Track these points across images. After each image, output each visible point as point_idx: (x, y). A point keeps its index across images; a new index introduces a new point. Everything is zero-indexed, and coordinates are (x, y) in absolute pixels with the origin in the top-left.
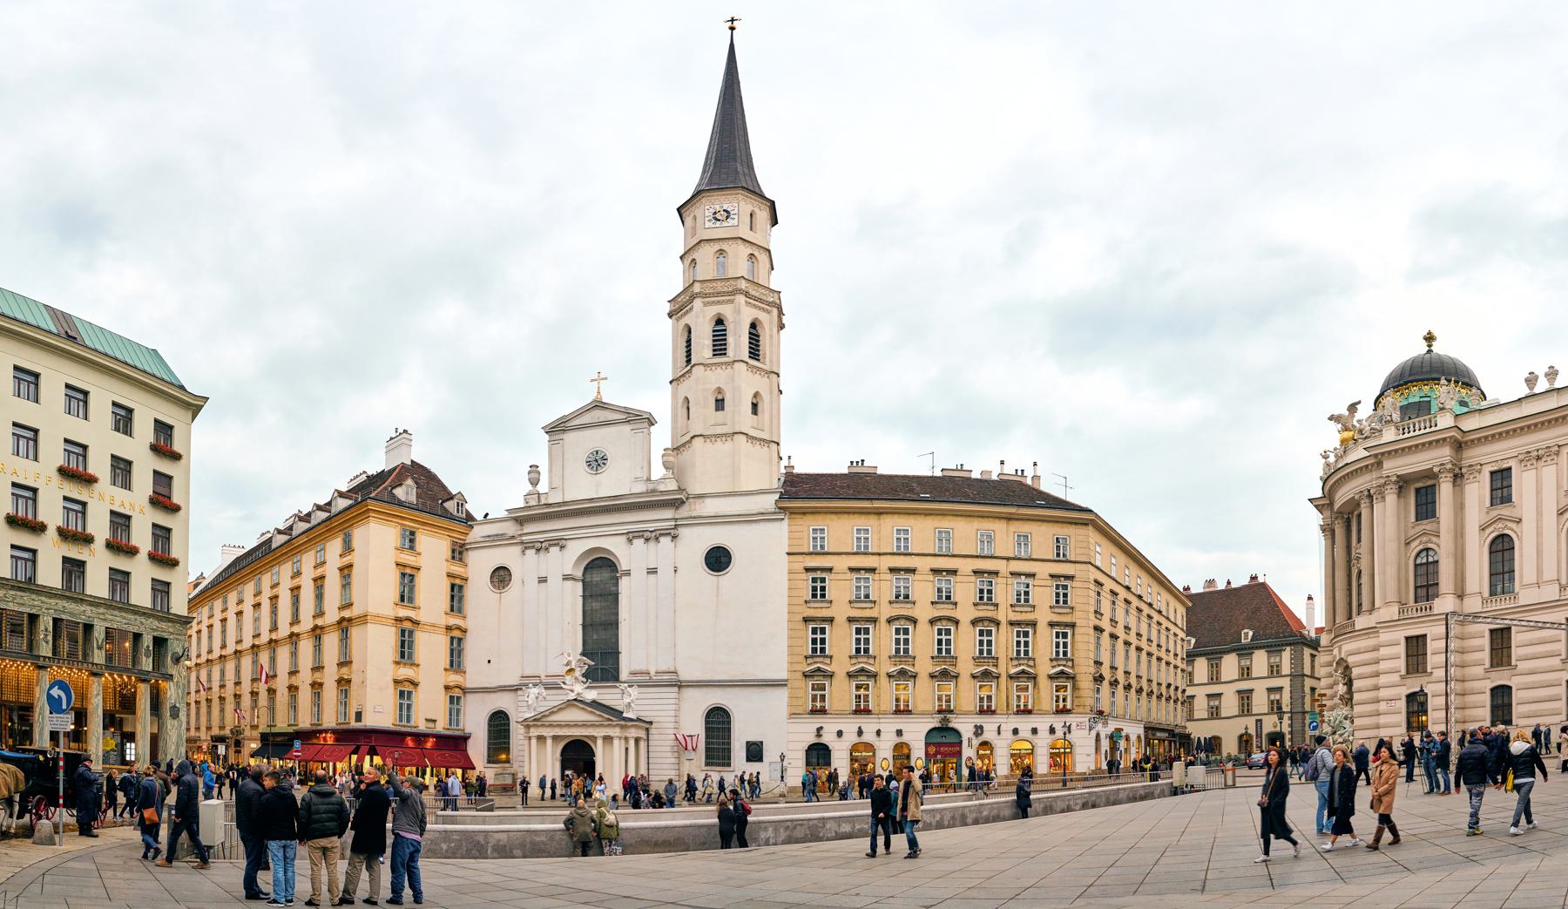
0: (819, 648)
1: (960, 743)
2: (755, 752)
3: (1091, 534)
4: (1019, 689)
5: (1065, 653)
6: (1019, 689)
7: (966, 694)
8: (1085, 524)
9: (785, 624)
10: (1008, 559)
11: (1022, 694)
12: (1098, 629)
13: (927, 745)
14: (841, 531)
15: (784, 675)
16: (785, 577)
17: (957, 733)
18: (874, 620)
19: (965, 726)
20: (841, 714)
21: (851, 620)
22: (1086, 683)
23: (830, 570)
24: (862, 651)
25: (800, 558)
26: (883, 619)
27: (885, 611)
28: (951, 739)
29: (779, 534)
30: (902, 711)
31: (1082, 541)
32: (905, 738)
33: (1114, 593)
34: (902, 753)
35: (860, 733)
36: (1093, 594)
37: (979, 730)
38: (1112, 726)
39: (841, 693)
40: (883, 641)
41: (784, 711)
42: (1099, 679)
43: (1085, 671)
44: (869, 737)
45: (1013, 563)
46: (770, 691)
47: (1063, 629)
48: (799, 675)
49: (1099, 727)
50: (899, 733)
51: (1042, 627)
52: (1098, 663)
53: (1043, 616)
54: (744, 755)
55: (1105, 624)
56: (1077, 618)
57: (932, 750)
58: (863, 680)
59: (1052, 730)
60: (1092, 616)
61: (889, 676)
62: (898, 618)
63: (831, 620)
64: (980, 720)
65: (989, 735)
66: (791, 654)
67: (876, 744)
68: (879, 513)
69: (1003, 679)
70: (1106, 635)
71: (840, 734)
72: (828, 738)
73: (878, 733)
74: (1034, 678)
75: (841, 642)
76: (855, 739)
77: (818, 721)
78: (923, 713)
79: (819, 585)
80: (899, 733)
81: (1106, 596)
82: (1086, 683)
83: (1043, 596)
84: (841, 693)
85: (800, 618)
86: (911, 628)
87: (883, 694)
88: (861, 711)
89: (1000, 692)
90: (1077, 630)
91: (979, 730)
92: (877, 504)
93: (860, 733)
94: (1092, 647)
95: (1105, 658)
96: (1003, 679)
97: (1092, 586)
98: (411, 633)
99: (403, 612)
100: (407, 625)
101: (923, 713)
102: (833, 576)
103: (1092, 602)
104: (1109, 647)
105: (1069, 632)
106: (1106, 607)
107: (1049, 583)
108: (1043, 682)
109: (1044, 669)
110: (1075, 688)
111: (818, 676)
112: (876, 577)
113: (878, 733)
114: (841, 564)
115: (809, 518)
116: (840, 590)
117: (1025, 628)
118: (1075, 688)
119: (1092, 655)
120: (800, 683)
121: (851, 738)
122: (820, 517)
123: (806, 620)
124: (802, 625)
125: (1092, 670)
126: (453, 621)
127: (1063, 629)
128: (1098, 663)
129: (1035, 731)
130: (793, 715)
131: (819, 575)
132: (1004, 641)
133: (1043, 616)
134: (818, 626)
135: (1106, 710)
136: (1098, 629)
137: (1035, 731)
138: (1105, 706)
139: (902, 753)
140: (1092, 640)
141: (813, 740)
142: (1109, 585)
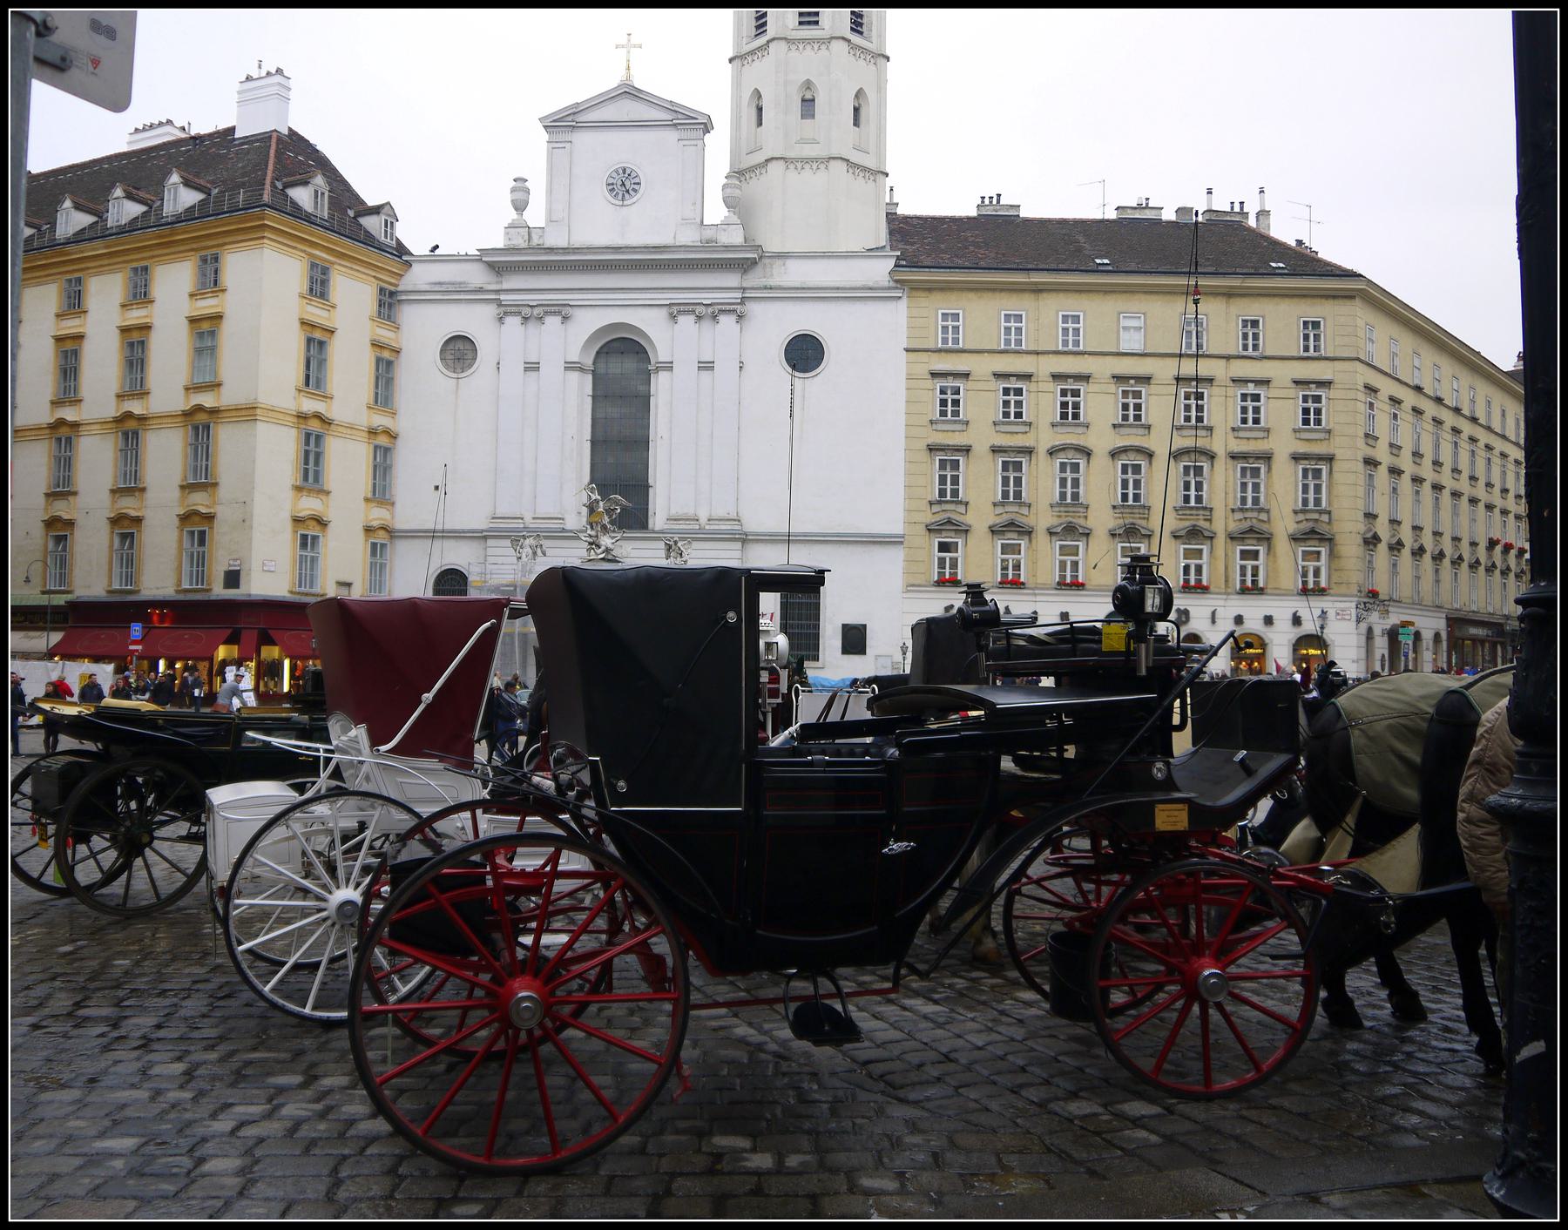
0: (949, 493)
2: (854, 639)
3: (1358, 314)
4: (1245, 555)
5: (1317, 501)
6: (1245, 555)
8: (1349, 296)
9: (902, 454)
11: (1249, 563)
12: (1371, 463)
14: (982, 317)
15: (897, 528)
16: (903, 384)
18: (1029, 451)
21: (996, 450)
22: (1351, 547)
23: (966, 375)
24: (1012, 493)
25: (924, 357)
27: (1045, 438)
29: (892, 323)
31: (1344, 324)
33: (1395, 401)
36: (1362, 407)
38: (1394, 619)
40: (1042, 481)
41: (898, 581)
42: (1372, 541)
43: (1349, 528)
46: (877, 550)
47: (1314, 465)
48: (921, 529)
49: (1374, 617)
51: (1281, 463)
52: (1370, 516)
53: (1283, 443)
54: (838, 643)
55: (1382, 453)
56: (1337, 447)
58: (1012, 539)
59: (1297, 620)
60: (1361, 442)
62: (1063, 449)
63: (967, 450)
66: (908, 498)
68: (1037, 290)
69: (1221, 540)
70: (1383, 471)
74: (1267, 539)
75: (981, 484)
79: (950, 397)
81: (1382, 405)
82: (1351, 547)
83: (1281, 412)
85: (923, 445)
89: (1219, 560)
90: (1337, 466)
92: (1036, 278)
94: (1361, 491)
95: (1382, 507)
96: (1221, 540)
97: (1361, 396)
98: (319, 438)
99: (310, 405)
100: (315, 426)
101: (1099, 589)
102: (970, 385)
103: (1361, 419)
104: (1387, 490)
105: (1324, 469)
106: (1382, 426)
107: (1291, 393)
108: (1282, 544)
110: (1332, 555)
112: (1033, 386)
114: (982, 367)
115: (937, 297)
116: (982, 405)
117: (1253, 463)
119: (1361, 504)
122: (953, 296)
123: (932, 449)
124: (925, 456)
125: (1361, 527)
126: (380, 420)
127: (1314, 465)
128: (1370, 516)
129: (1269, 620)
130: (911, 587)
131: (950, 383)
132: (1222, 484)
133: (1283, 443)
134: (949, 458)
135: (1384, 593)
136: (1371, 463)
137: (1269, 620)
138: (1382, 585)
140: (1361, 480)
142: (1387, 388)
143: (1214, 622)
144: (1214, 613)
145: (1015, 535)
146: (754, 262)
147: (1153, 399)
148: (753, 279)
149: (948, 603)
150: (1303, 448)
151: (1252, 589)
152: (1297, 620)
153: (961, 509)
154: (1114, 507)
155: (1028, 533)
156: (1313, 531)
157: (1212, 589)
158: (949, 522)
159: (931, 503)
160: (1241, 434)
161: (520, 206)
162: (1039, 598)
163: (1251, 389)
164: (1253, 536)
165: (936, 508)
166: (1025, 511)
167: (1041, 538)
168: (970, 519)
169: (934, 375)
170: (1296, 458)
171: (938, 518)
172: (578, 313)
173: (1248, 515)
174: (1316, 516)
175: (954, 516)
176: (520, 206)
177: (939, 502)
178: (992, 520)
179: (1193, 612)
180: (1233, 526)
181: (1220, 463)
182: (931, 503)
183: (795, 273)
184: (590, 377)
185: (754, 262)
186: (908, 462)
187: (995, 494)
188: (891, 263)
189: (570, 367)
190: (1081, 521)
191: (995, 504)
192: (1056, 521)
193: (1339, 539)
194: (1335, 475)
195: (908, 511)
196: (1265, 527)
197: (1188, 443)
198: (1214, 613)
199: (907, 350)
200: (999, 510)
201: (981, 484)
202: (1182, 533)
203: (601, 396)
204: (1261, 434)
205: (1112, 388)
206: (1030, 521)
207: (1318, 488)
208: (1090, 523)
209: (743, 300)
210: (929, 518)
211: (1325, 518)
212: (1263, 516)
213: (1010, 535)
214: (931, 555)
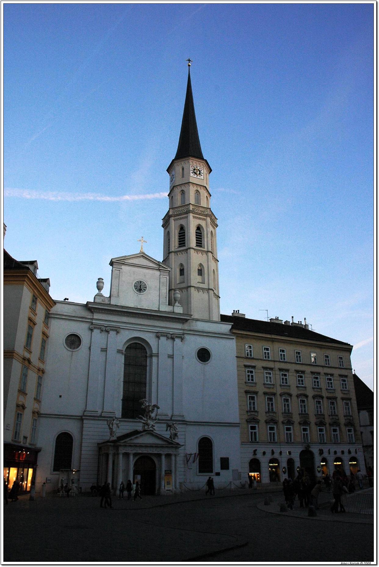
2: (225, 463)
10: (323, 366)
14: (257, 348)
15: (238, 421)
17: (312, 453)
18: (274, 394)
19: (315, 450)
21: (265, 394)
25: (242, 360)
26: (278, 393)
30: (289, 442)
32: (292, 456)
34: (290, 462)
35: (273, 453)
37: (321, 452)
39: (262, 431)
44: (276, 456)
45: (325, 369)
51: (339, 399)
54: (219, 465)
59: (350, 452)
61: (283, 423)
64: (321, 447)
65: (325, 455)
66: (241, 410)
67: (280, 459)
69: (328, 425)
71: (264, 453)
72: (259, 456)
73: (281, 453)
74: (338, 425)
77: (255, 447)
80: (290, 453)
84: (262, 431)
85: (243, 391)
87: (281, 432)
88: (272, 441)
91: (321, 452)
93: (273, 453)
96: (328, 425)
107: (338, 378)
108: (343, 428)
111: (252, 420)
113: (281, 453)
121: (269, 456)
123: (247, 392)
124: (244, 394)
129: (343, 452)
130: (243, 443)
137: (343, 452)
141: (251, 456)
143: (329, 453)
144: (329, 450)
145: (273, 424)
146: (186, 320)
147: (306, 379)
148: (186, 326)
149: (255, 449)
152: (350, 452)
153: (256, 414)
154: (299, 414)
155: (276, 423)
158: (254, 419)
159: (247, 412)
161: (99, 288)
163: (329, 377)
165: (249, 414)
168: (259, 418)
169: (246, 366)
170: (343, 399)
172: (122, 331)
174: (349, 418)
176: (99, 288)
177: (250, 411)
181: (325, 399)
182: (247, 412)
183: (200, 326)
184: (123, 356)
185: (186, 320)
186: (240, 397)
188: (230, 327)
189: (119, 351)
191: (266, 413)
195: (240, 415)
197: (316, 393)
198: (329, 450)
199: (237, 357)
200: (268, 415)
201: (261, 404)
203: (127, 365)
209: (184, 334)
210: (246, 417)
211: (351, 418)
213: (271, 424)
214: (248, 431)
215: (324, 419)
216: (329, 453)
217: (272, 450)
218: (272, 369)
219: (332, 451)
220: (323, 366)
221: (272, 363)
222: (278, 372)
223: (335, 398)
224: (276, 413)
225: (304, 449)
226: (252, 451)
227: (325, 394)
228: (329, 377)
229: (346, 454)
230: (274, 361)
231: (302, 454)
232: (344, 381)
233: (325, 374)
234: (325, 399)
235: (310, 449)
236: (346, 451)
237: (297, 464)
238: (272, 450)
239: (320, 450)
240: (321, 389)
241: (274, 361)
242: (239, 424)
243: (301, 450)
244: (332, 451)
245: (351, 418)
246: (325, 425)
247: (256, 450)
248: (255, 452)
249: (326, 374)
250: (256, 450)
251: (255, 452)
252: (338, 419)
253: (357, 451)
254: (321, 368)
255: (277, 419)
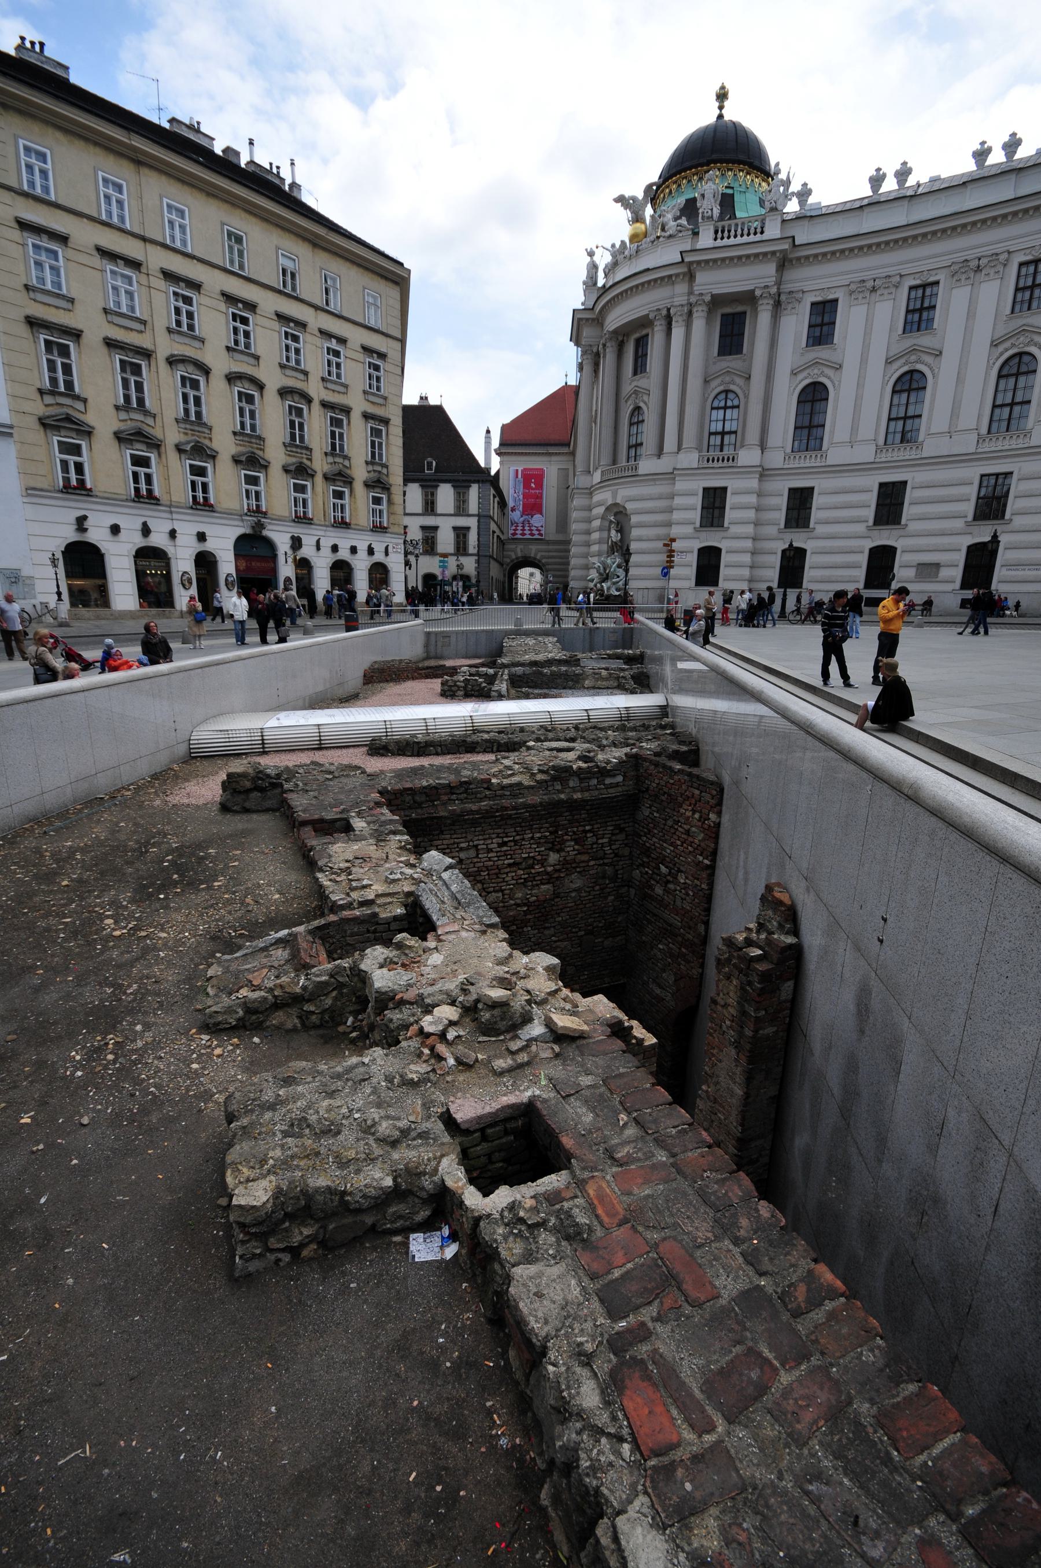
1: (274, 557)
5: (380, 455)
7: (277, 492)
10: (316, 308)
13: (237, 556)
17: (270, 545)
19: (280, 538)
20: (111, 500)
24: (133, 402)
28: (263, 551)
30: (202, 505)
32: (210, 545)
34: (205, 562)
35: (146, 531)
37: (296, 543)
39: (107, 464)
44: (158, 539)
45: (322, 316)
50: (201, 537)
51: (356, 416)
57: (243, 565)
59: (371, 551)
61: (179, 449)
64: (298, 530)
65: (307, 551)
66: (10, 379)
67: (170, 551)
69: (319, 479)
71: (115, 530)
72: (97, 535)
73: (173, 534)
74: (349, 482)
75: (98, 380)
76: (139, 541)
78: (229, 513)
80: (201, 537)
84: (107, 464)
85: (19, 315)
86: (202, 381)
87: (172, 475)
88: (145, 497)
91: (296, 543)
96: (319, 479)
101: (229, 513)
107: (361, 356)
109: (360, 473)
110: (390, 502)
113: (173, 534)
117: (338, 413)
118: (390, 502)
120: (37, 435)
129: (354, 550)
137: (354, 550)
139: (205, 562)
141: (71, 535)
143: (318, 548)
144: (318, 542)
145: (143, 447)
150: (371, 409)
151: (343, 524)
152: (371, 551)
154: (235, 433)
155: (156, 445)
156: (379, 481)
157: (315, 521)
158: (68, 419)
160: (330, 385)
162: (175, 516)
164: (340, 478)
166: (150, 421)
167: (172, 456)
170: (366, 416)
171: (51, 411)
173: (338, 460)
174: (379, 468)
175: (71, 412)
177: (53, 393)
178: (116, 426)
179: (305, 540)
180: (326, 468)
181: (316, 406)
182: (41, 392)
187: (116, 396)
190: (207, 442)
192: (183, 438)
193: (393, 490)
194: (390, 437)
196: (348, 472)
198: (318, 542)
202: (292, 468)
204: (342, 389)
205: (222, 306)
206: (157, 433)
207: (380, 444)
208: (215, 445)
210: (40, 410)
211: (385, 471)
212: (346, 463)
215: (310, 460)
216: (318, 548)
217: (145, 524)
218: (135, 265)
219: (326, 544)
220: (316, 308)
221: (139, 244)
222: (160, 283)
223: (347, 411)
224: (154, 416)
225: (248, 531)
226: (73, 520)
227: (315, 389)
228: (334, 344)
229: (362, 553)
230: (144, 239)
231: (242, 542)
232: (377, 368)
233: (321, 331)
234: (316, 406)
235: (265, 533)
236: (362, 547)
237: (227, 566)
238: (145, 524)
239: (293, 538)
240: (306, 373)
241: (144, 239)
242: (11, 427)
243: (240, 531)
244: (326, 544)
245: (385, 471)
246: (313, 476)
247: (85, 518)
248: (81, 521)
249: (325, 334)
250: (85, 518)
251: (81, 521)
252: (350, 468)
253: (390, 549)
254: (311, 311)
255: (160, 436)
